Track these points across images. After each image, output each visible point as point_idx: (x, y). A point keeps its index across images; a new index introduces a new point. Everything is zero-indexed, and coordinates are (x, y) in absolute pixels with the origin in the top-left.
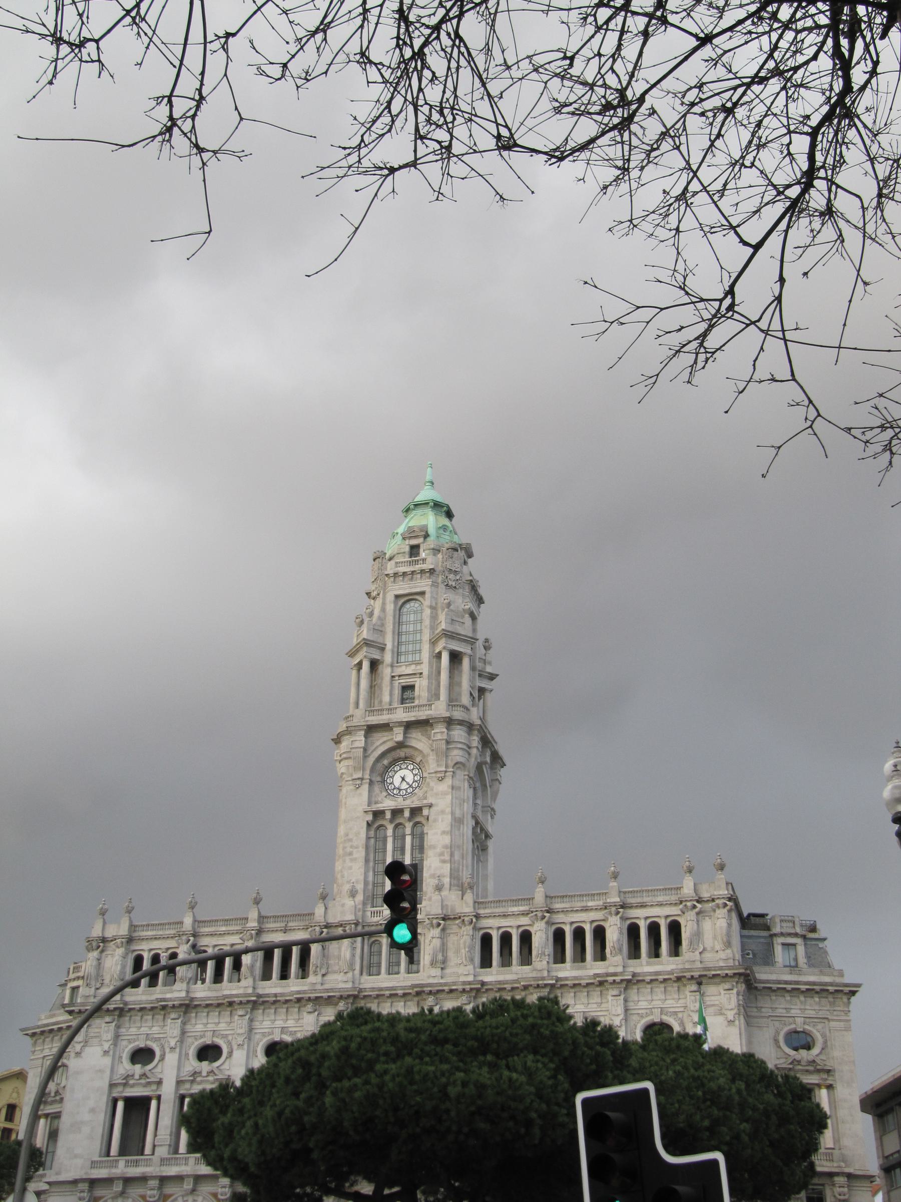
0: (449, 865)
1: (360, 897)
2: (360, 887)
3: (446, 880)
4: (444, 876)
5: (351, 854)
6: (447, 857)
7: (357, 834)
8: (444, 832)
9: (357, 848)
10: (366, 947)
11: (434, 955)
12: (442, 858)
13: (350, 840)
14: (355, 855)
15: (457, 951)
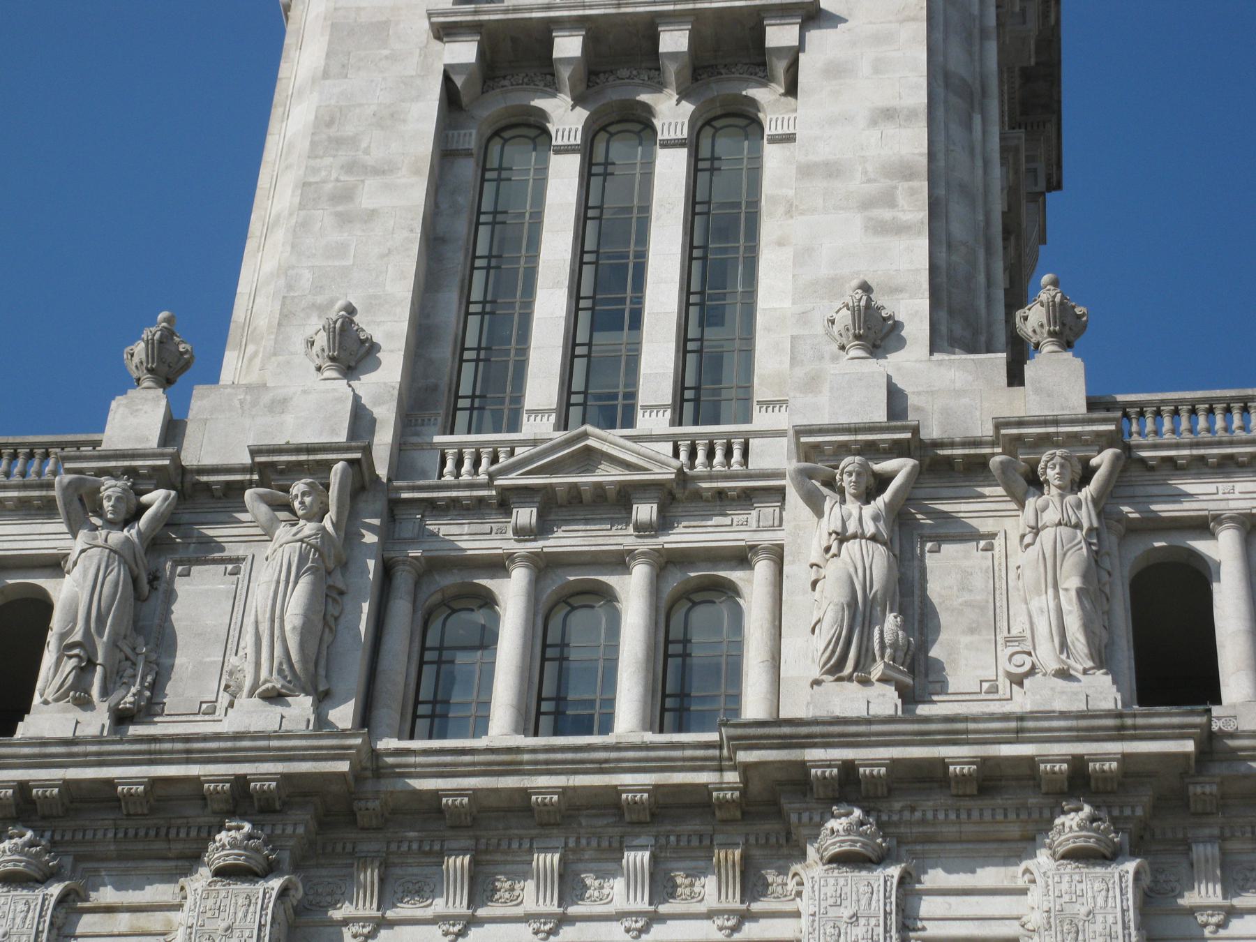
0: (924, 242)
1: (390, 371)
2: (390, 329)
3: (912, 310)
4: (895, 290)
5: (344, 195)
6: (914, 210)
7: (388, 119)
8: (887, 115)
9: (377, 171)
10: (401, 610)
11: (860, 614)
12: (886, 214)
13: (339, 142)
14: (369, 196)
15: (993, 615)
